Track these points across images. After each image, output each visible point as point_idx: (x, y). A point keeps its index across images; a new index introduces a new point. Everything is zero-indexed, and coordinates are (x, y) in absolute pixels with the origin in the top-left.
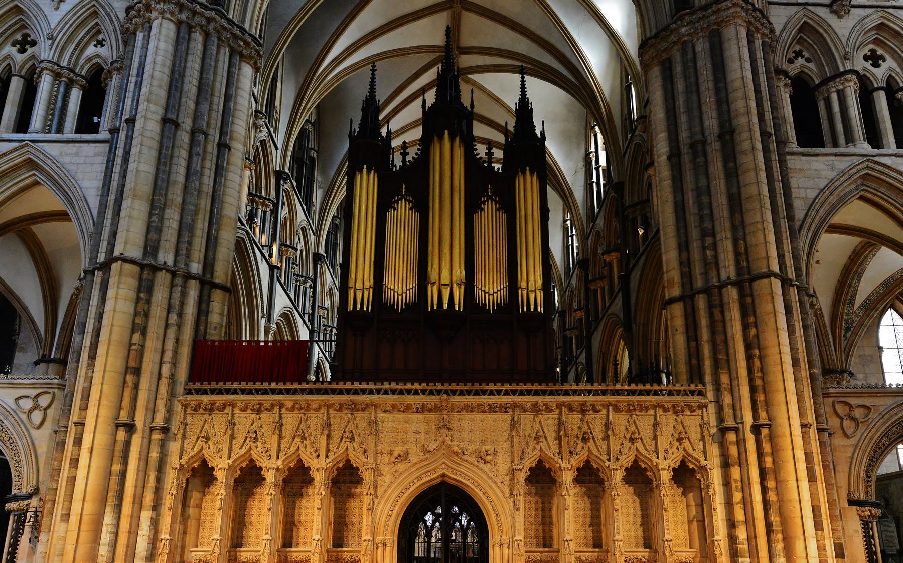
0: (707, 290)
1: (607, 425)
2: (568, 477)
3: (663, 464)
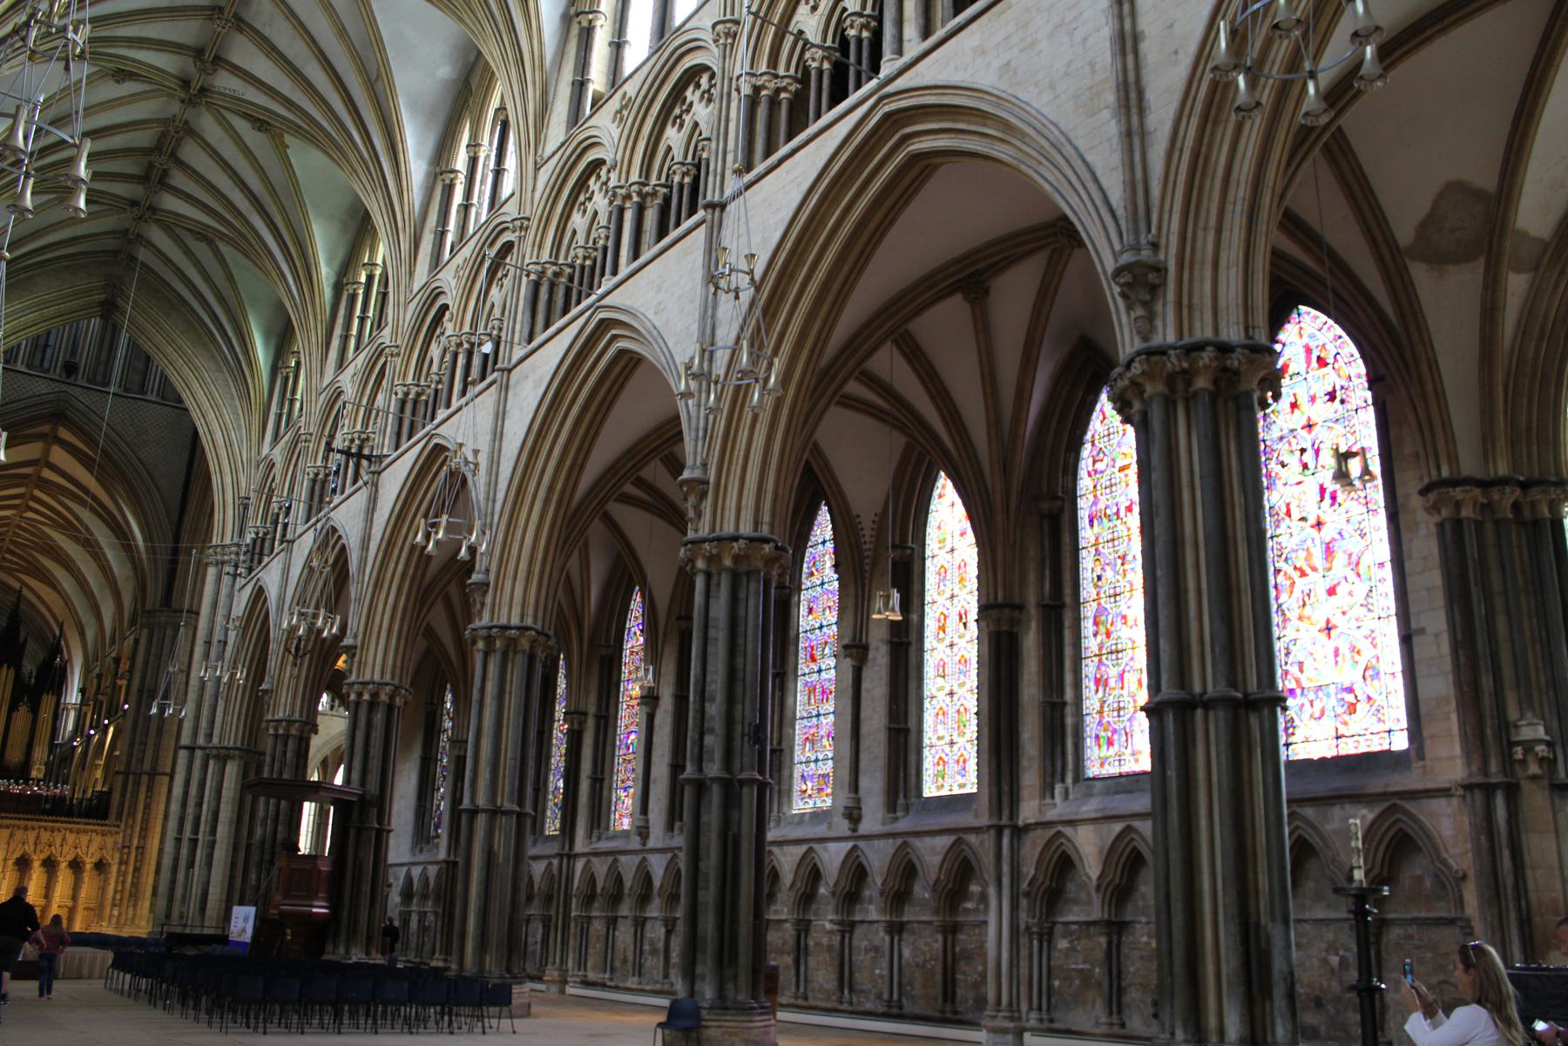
0: (135, 774)
1: (64, 839)
2: (36, 864)
3: (88, 860)
